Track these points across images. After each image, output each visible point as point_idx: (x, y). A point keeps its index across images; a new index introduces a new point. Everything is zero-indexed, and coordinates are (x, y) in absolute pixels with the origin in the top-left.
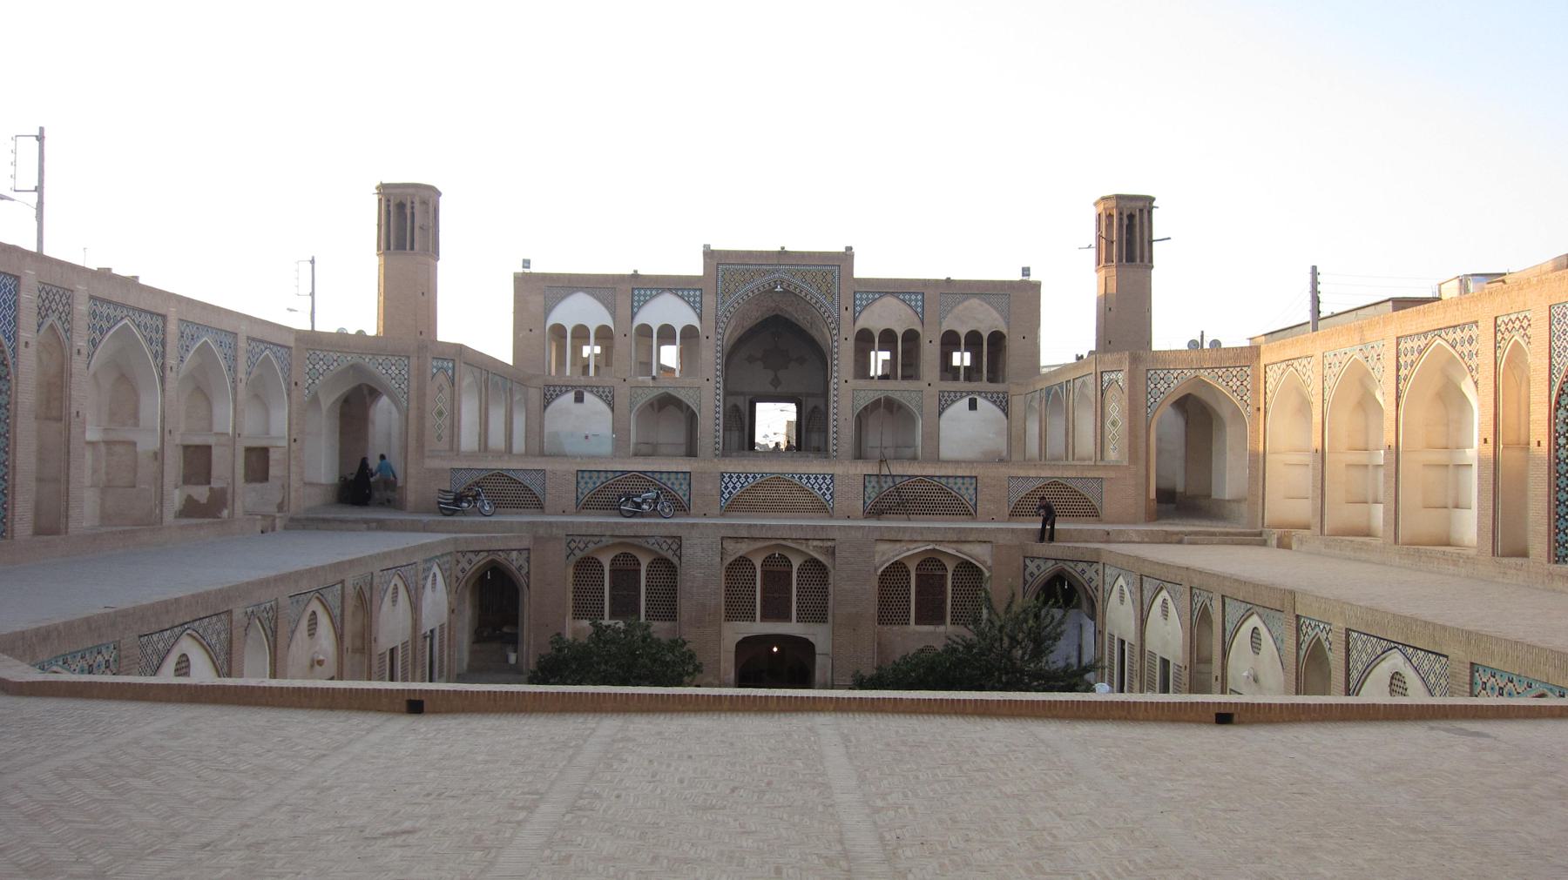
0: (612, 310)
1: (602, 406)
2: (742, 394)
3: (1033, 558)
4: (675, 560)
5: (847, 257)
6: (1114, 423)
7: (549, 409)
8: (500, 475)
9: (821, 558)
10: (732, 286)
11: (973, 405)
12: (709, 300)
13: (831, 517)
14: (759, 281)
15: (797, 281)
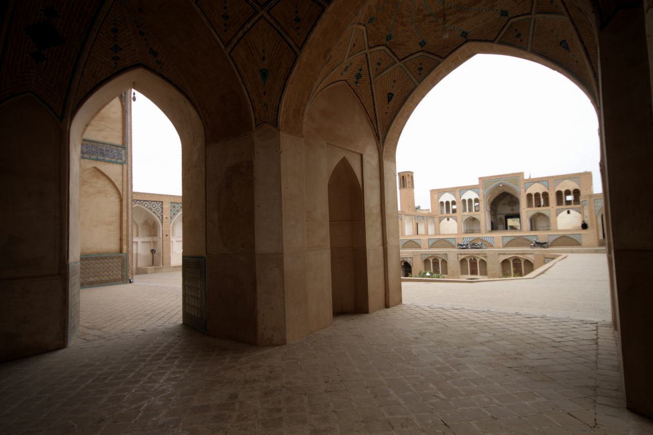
0: (455, 196)
1: (455, 221)
2: (503, 214)
3: (547, 258)
4: (446, 260)
5: (522, 174)
6: (587, 217)
7: (442, 222)
8: (411, 241)
9: (484, 259)
10: (487, 186)
11: (569, 212)
12: (481, 191)
13: (494, 248)
14: (495, 184)
15: (506, 182)
